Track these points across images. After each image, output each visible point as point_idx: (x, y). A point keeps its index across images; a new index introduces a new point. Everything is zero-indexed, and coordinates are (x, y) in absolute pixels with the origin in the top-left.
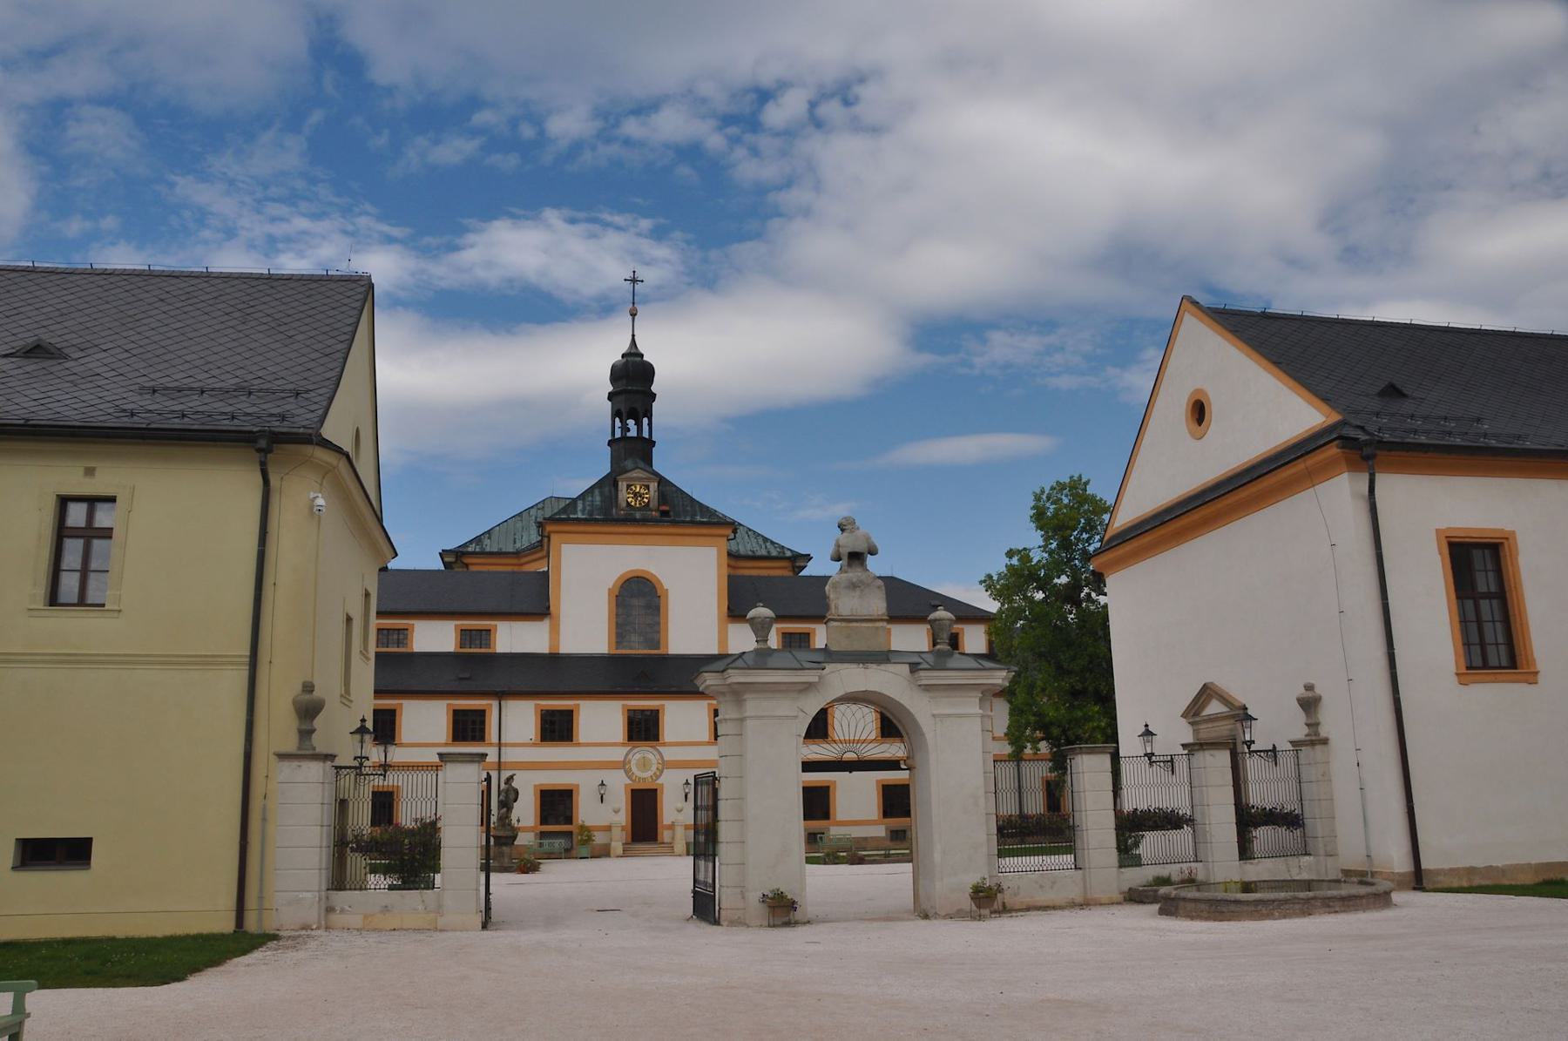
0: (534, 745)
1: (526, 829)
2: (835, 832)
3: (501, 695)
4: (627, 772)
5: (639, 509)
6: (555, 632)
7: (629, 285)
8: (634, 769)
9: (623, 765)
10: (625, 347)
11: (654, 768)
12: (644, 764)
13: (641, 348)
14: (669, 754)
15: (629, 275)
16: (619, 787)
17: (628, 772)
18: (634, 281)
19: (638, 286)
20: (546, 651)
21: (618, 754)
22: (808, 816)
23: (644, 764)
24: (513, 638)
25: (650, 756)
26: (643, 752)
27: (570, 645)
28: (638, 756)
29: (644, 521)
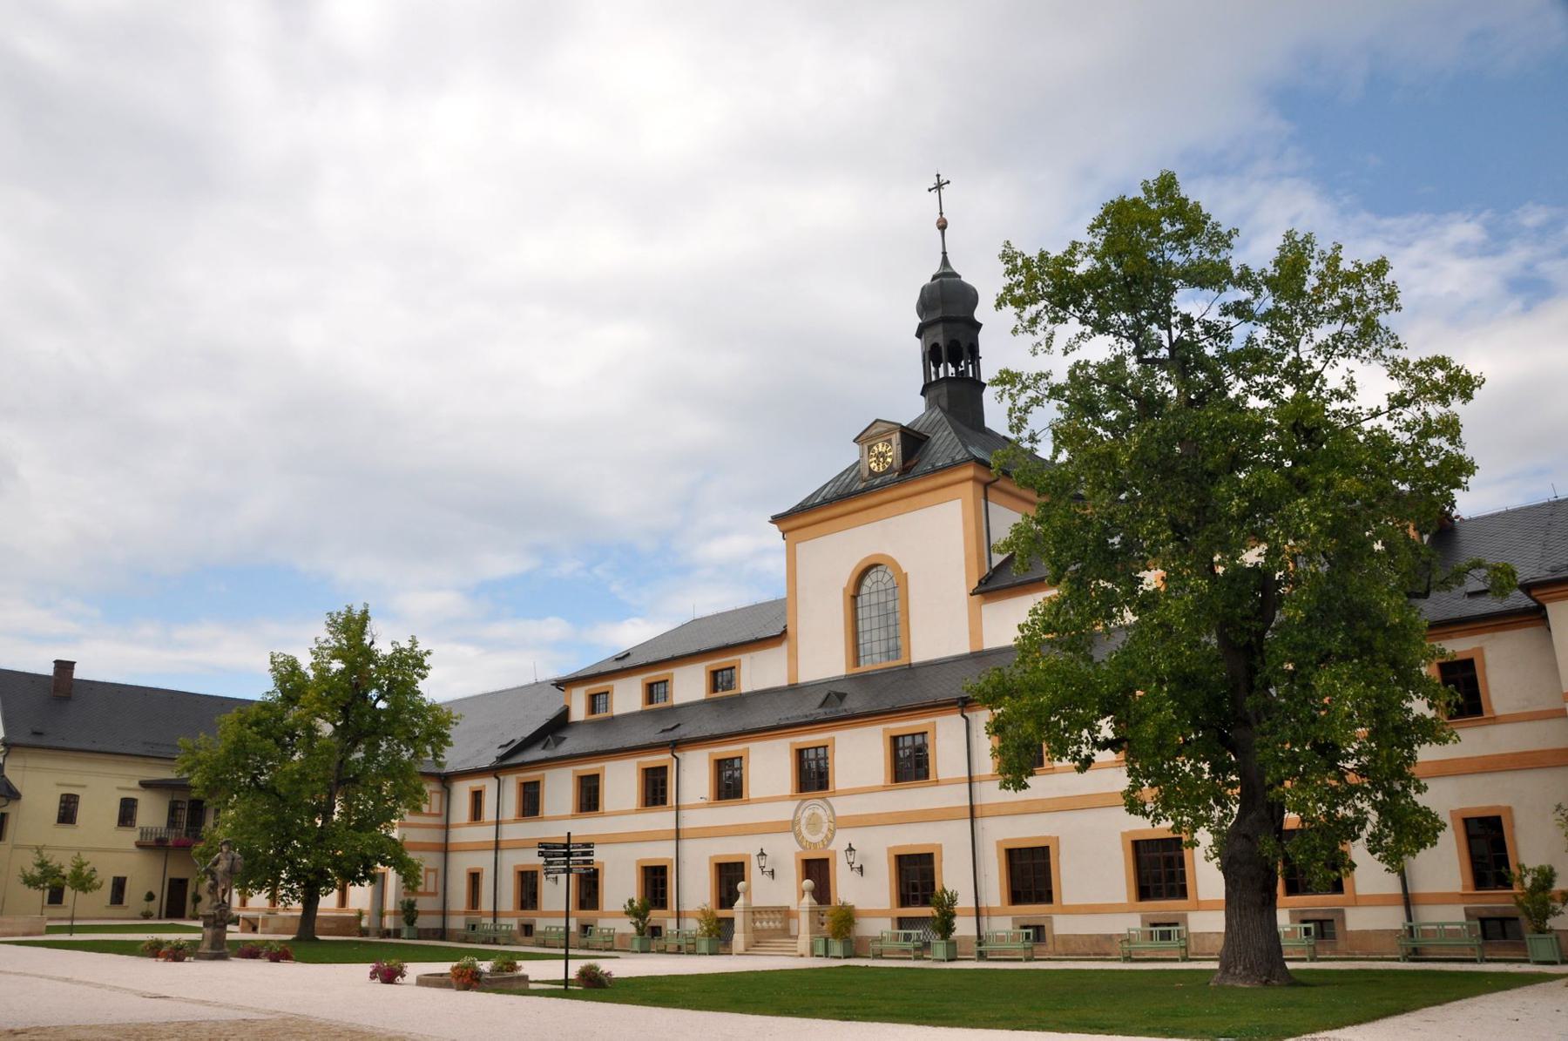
0: (709, 805)
1: (458, 913)
2: (1061, 926)
3: (675, 746)
4: (797, 836)
5: (883, 474)
6: (793, 657)
7: (935, 194)
8: (805, 832)
9: (791, 827)
10: (936, 268)
11: (825, 830)
12: (814, 823)
13: (956, 266)
14: (843, 807)
15: (933, 182)
16: (787, 853)
17: (799, 837)
18: (939, 186)
19: (945, 190)
20: (785, 683)
21: (785, 812)
22: (1144, 891)
23: (814, 823)
24: (759, 673)
25: (820, 812)
26: (814, 805)
27: (810, 672)
28: (807, 813)
29: (883, 487)
